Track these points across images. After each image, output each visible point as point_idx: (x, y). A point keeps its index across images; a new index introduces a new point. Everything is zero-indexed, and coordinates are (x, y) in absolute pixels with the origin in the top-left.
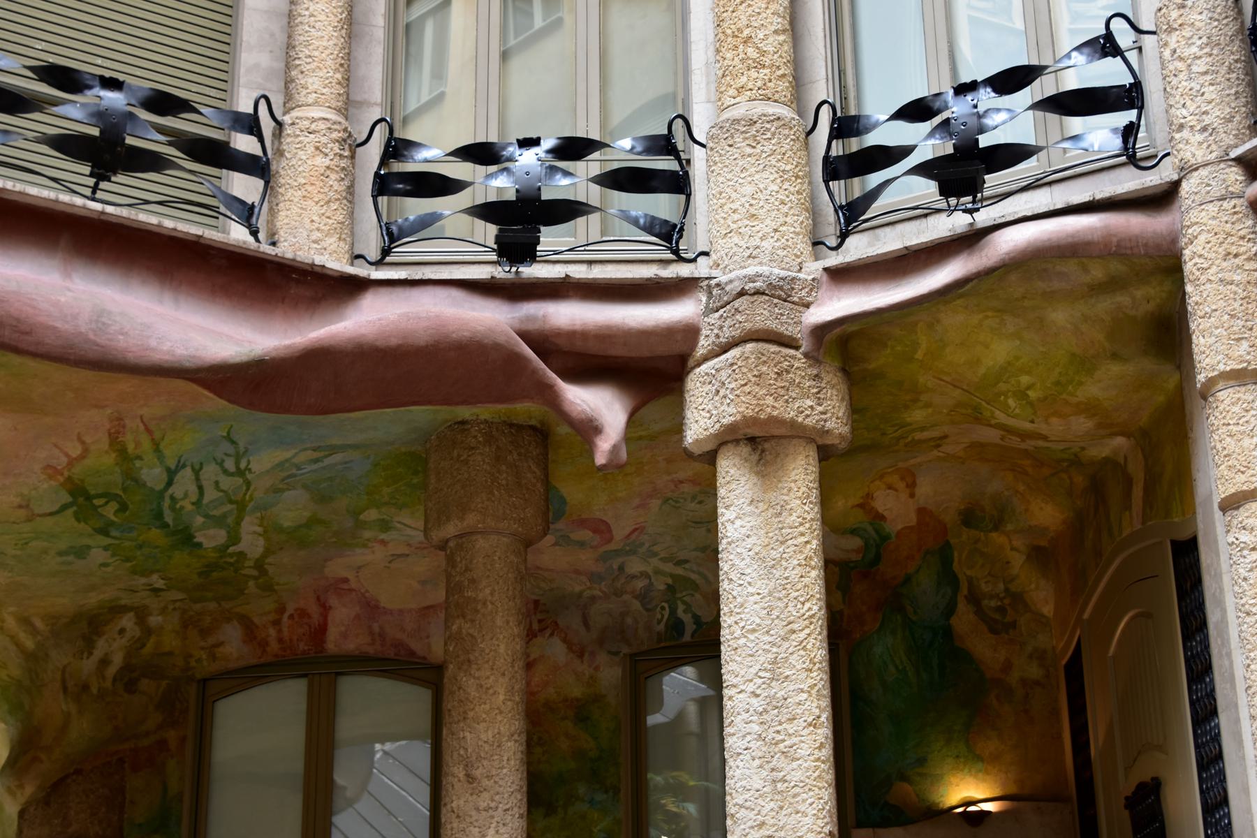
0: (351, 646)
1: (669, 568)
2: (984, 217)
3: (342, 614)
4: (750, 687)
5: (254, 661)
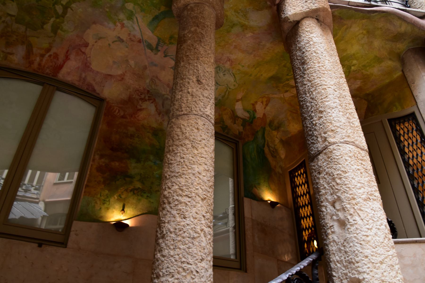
0: (69, 79)
5: (23, 68)
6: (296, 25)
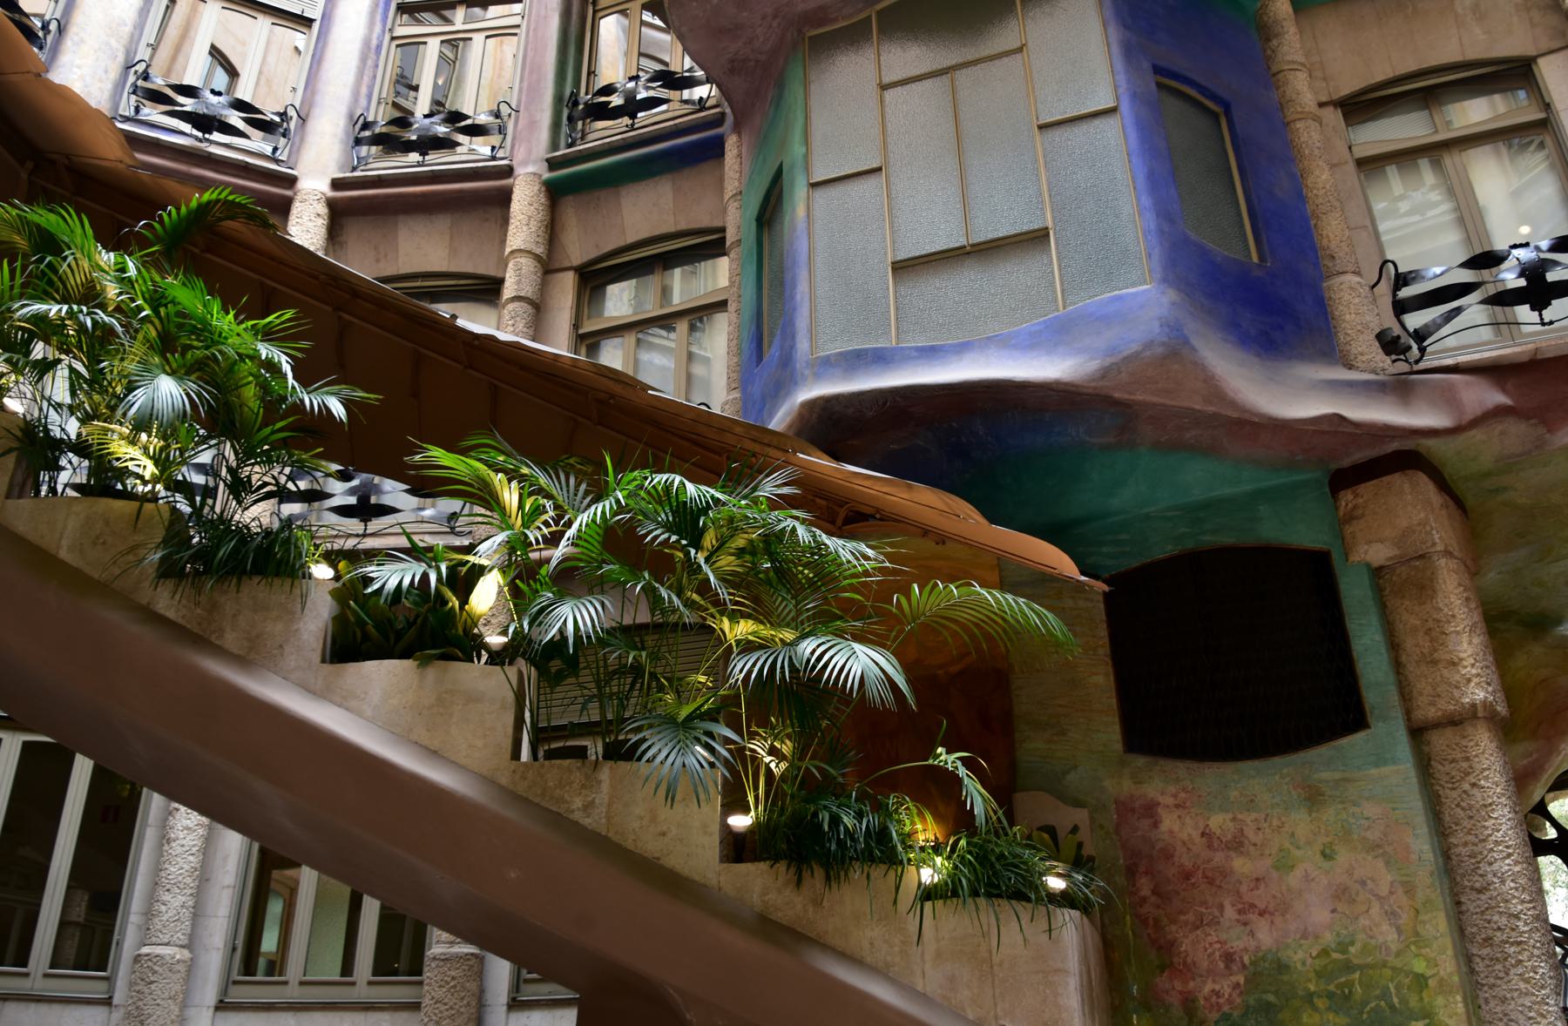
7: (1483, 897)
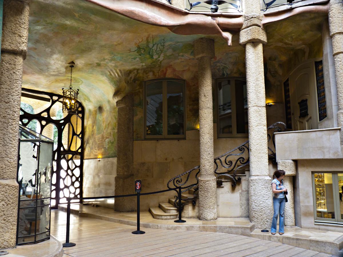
0: (170, 76)
1: (223, 65)
2: (294, 6)
3: (169, 71)
4: (253, 82)
5: (154, 79)
6: (244, 45)
7: (7, 105)
